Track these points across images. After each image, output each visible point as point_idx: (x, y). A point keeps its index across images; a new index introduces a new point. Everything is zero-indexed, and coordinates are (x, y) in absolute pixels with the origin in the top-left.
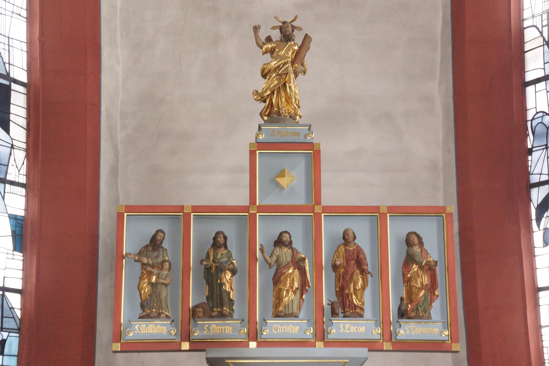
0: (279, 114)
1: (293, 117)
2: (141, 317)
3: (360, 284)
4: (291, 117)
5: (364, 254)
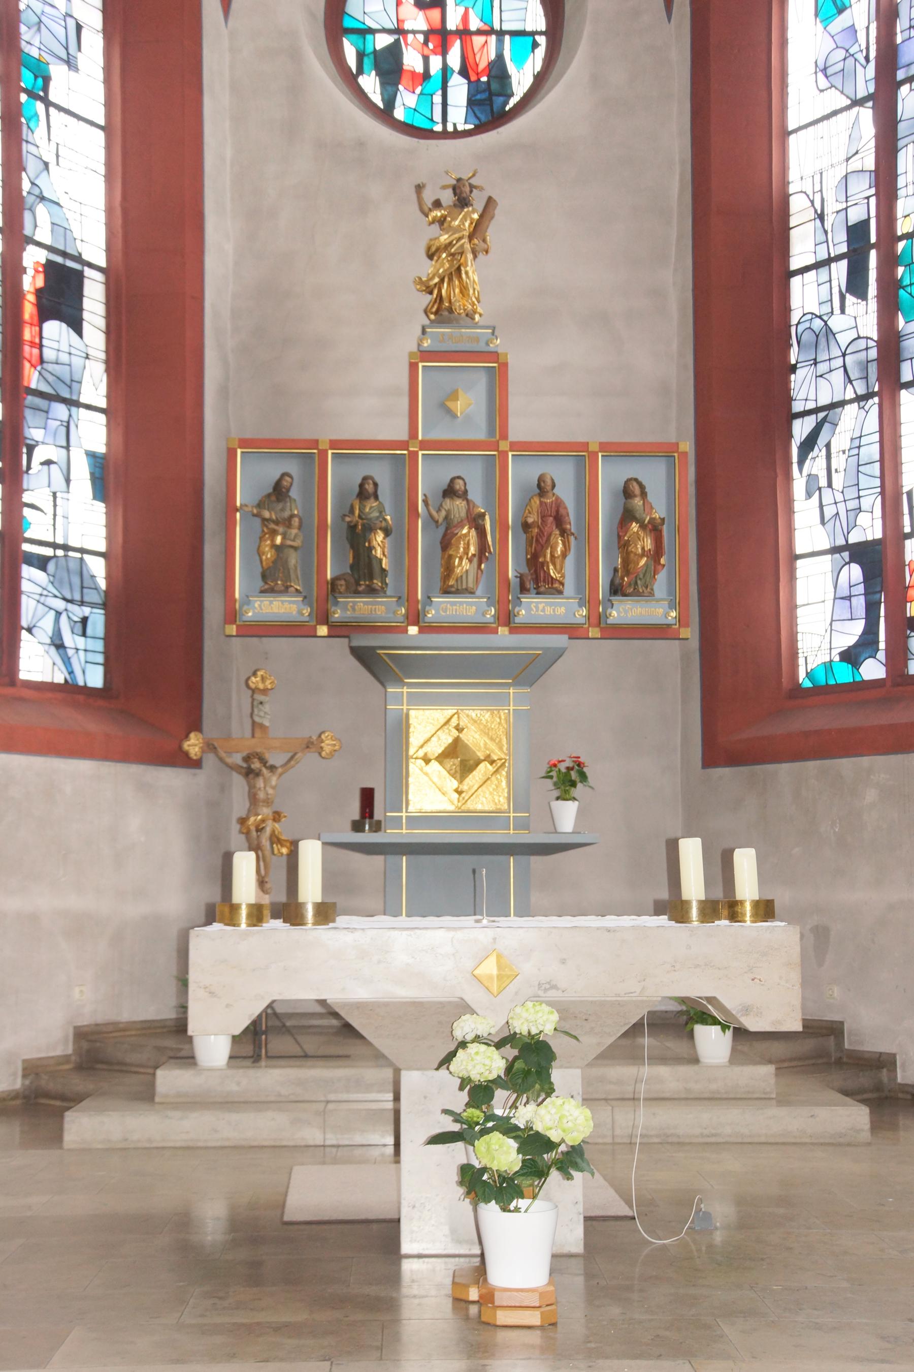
0: (450, 310)
1: (470, 316)
2: (262, 592)
3: (559, 549)
4: (467, 315)
5: (566, 508)
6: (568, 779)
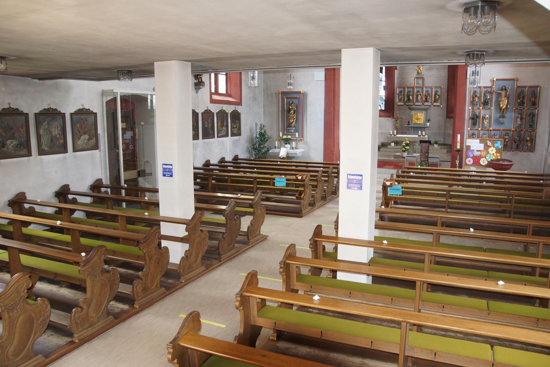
6: (429, 121)
